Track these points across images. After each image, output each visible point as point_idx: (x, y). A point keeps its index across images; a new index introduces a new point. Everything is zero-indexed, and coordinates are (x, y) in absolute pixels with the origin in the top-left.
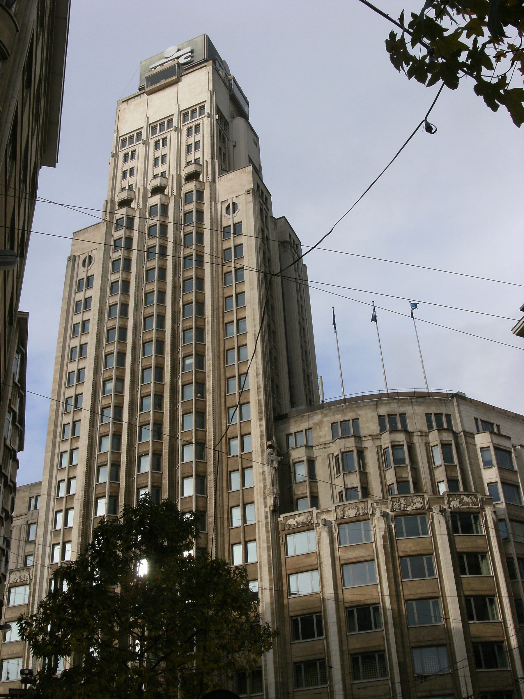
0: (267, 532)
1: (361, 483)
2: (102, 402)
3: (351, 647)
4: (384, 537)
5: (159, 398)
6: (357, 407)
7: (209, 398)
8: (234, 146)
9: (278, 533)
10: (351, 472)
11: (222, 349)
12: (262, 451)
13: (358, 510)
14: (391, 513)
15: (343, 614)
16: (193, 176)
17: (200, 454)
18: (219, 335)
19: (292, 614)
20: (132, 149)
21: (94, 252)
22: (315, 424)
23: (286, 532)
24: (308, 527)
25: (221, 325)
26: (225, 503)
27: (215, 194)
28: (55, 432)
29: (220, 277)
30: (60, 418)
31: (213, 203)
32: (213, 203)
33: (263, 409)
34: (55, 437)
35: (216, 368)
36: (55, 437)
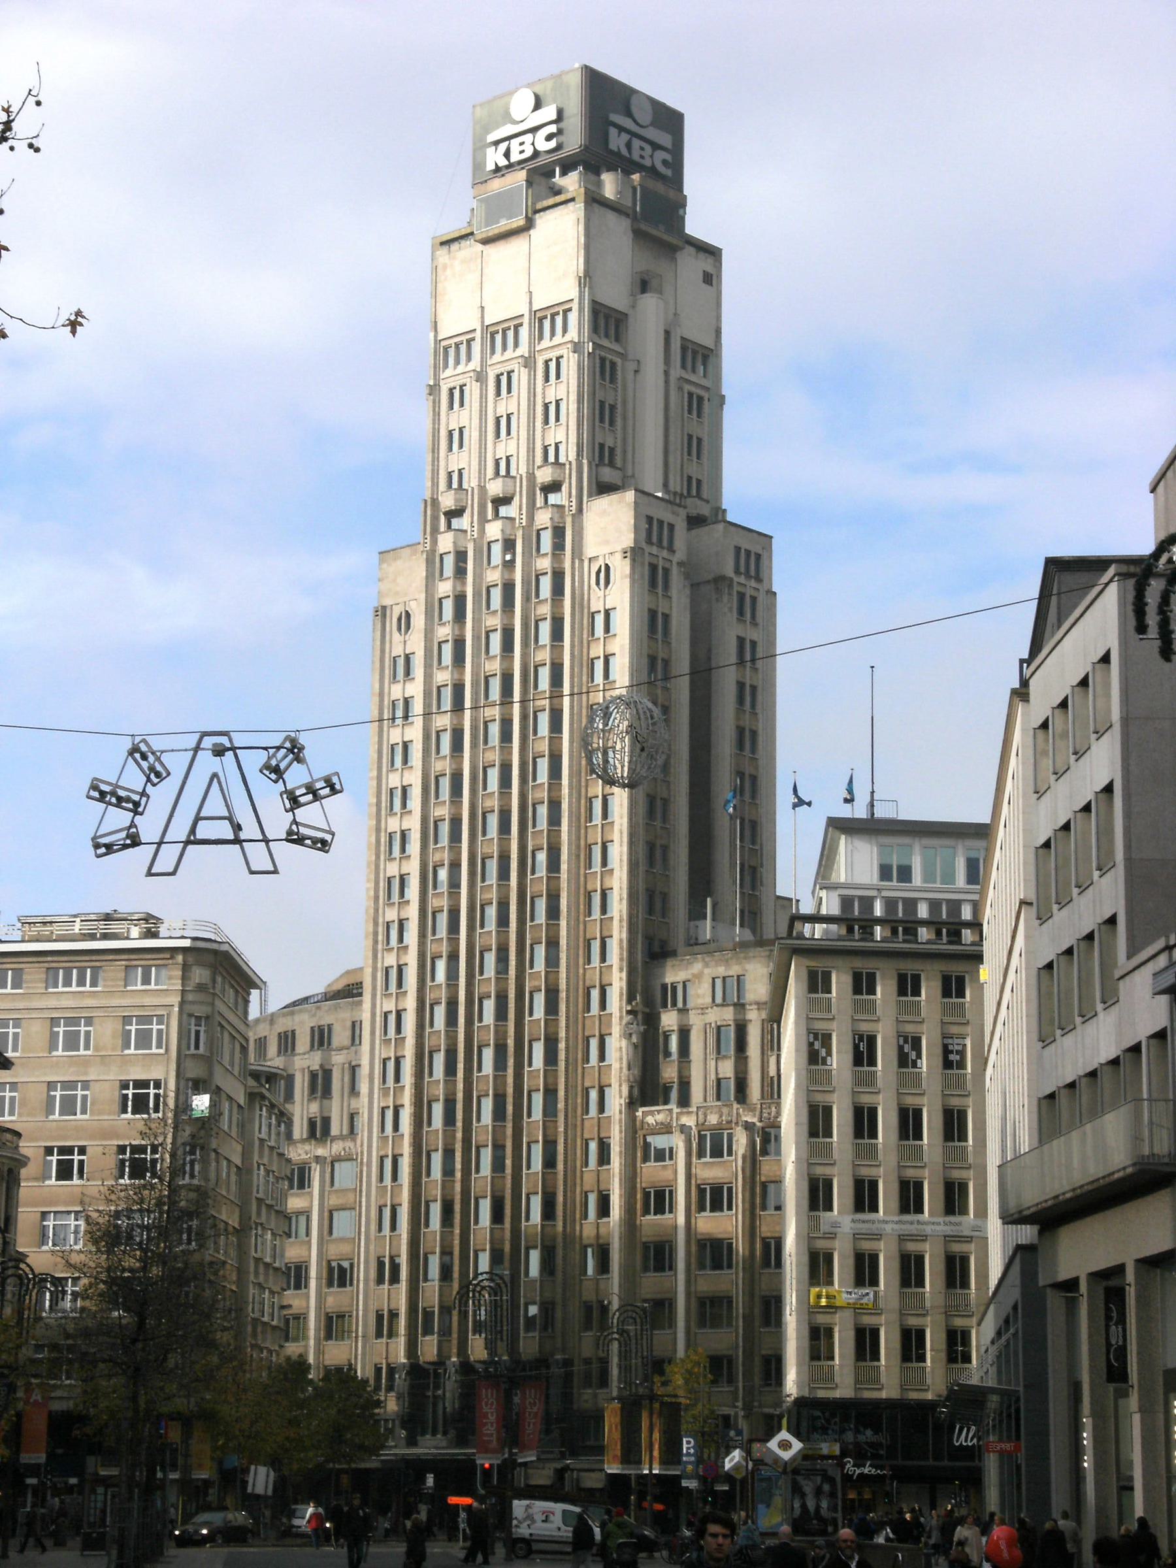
0: (621, 1132)
1: (737, 1072)
2: (433, 903)
3: (700, 1288)
4: (744, 1157)
5: (503, 906)
6: (745, 958)
7: (563, 923)
8: (636, 372)
9: (635, 1132)
10: (725, 1057)
11: (582, 843)
12: (621, 1018)
13: (721, 1116)
14: (758, 1124)
15: (694, 1249)
17: (552, 1007)
18: (579, 819)
19: (644, 1239)
20: (461, 382)
22: (694, 976)
23: (644, 1132)
24: (666, 1129)
25: (583, 801)
26: (579, 1082)
27: (582, 538)
28: (376, 934)
30: (381, 911)
31: (577, 561)
32: (577, 561)
34: (376, 942)
35: (575, 876)
36: (376, 942)
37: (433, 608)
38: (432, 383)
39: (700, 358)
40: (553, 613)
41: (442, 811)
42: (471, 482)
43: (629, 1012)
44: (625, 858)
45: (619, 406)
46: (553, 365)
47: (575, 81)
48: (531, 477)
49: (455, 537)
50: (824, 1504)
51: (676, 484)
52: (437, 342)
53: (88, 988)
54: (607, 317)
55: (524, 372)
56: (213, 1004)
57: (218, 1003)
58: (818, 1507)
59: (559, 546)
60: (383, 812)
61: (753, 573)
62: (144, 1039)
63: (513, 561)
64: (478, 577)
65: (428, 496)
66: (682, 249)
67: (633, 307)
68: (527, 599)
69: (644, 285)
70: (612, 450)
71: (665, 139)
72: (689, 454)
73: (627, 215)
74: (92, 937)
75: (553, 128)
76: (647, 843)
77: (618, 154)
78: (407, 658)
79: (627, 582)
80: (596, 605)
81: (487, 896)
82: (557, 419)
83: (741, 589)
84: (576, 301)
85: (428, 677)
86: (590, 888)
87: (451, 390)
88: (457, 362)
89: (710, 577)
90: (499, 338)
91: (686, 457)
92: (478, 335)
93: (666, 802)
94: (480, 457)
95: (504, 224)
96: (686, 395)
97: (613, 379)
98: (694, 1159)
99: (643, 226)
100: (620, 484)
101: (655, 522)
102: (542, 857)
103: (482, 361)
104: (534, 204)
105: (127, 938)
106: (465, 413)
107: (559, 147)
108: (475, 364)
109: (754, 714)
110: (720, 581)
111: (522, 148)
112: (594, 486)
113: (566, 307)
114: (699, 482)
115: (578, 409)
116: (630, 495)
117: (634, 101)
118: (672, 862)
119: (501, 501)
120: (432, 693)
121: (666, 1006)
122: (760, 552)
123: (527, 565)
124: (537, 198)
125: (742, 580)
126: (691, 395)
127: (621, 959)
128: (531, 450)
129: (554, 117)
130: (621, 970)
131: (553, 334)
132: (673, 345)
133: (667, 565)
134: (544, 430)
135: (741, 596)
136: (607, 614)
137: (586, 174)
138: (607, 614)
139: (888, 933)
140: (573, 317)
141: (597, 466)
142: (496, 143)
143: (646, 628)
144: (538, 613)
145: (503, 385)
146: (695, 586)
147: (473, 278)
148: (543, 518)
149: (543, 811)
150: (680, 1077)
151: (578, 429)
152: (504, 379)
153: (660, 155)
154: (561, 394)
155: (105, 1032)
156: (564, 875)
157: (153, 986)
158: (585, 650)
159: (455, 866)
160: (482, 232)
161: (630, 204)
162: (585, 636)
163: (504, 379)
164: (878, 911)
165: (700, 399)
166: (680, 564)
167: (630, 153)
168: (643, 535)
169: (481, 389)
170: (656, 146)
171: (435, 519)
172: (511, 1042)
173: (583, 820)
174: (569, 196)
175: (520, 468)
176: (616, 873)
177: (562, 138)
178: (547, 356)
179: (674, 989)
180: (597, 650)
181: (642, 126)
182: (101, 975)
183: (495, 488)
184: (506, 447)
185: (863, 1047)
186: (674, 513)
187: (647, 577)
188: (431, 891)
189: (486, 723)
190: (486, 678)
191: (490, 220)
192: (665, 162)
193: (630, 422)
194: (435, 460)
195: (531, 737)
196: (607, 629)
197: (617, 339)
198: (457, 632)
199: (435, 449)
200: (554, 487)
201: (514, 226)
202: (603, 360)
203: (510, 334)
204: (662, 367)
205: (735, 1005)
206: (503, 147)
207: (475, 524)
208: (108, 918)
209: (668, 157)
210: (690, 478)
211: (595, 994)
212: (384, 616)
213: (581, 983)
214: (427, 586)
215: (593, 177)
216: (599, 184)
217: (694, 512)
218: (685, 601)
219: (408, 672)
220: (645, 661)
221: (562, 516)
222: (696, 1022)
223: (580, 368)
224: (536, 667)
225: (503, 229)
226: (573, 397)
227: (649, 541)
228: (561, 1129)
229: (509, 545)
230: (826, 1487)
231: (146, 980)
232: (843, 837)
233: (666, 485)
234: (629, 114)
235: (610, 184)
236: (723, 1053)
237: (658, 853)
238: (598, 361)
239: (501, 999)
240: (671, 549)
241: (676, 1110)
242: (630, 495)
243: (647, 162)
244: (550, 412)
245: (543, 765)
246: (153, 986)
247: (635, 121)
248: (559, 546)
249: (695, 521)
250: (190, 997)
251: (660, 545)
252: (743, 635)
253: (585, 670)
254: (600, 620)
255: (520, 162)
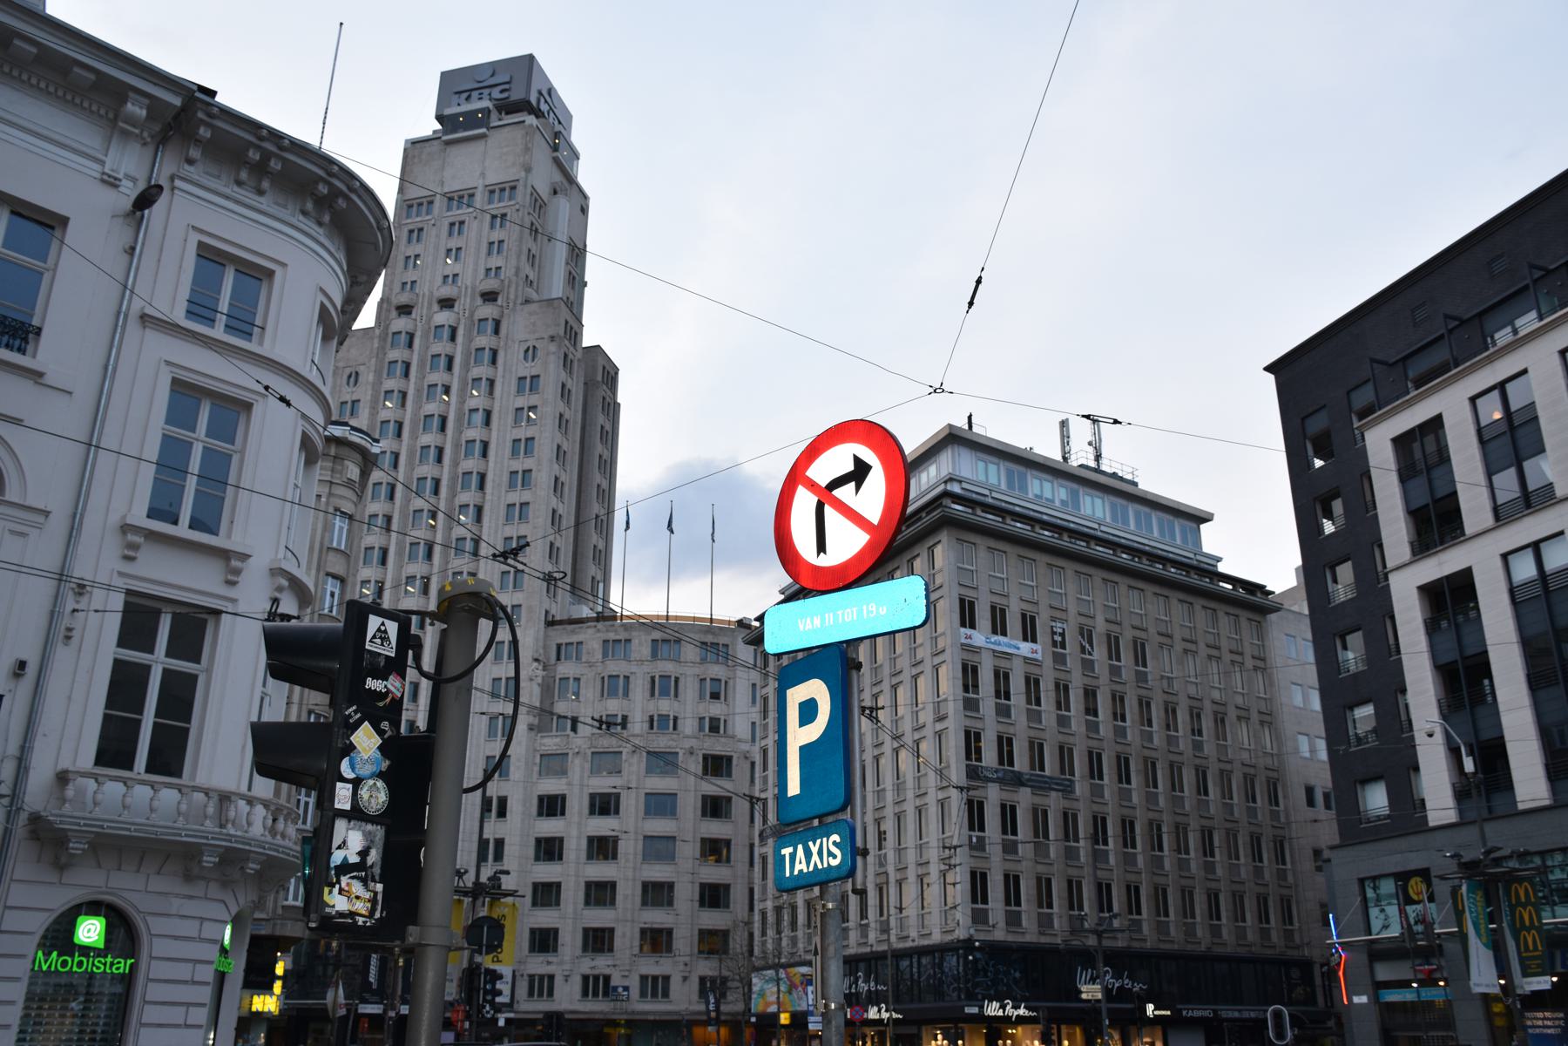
16: (489, 297)
21: (362, 368)
45: (538, 257)
69: (555, 192)
75: (507, 86)
165: (574, 278)
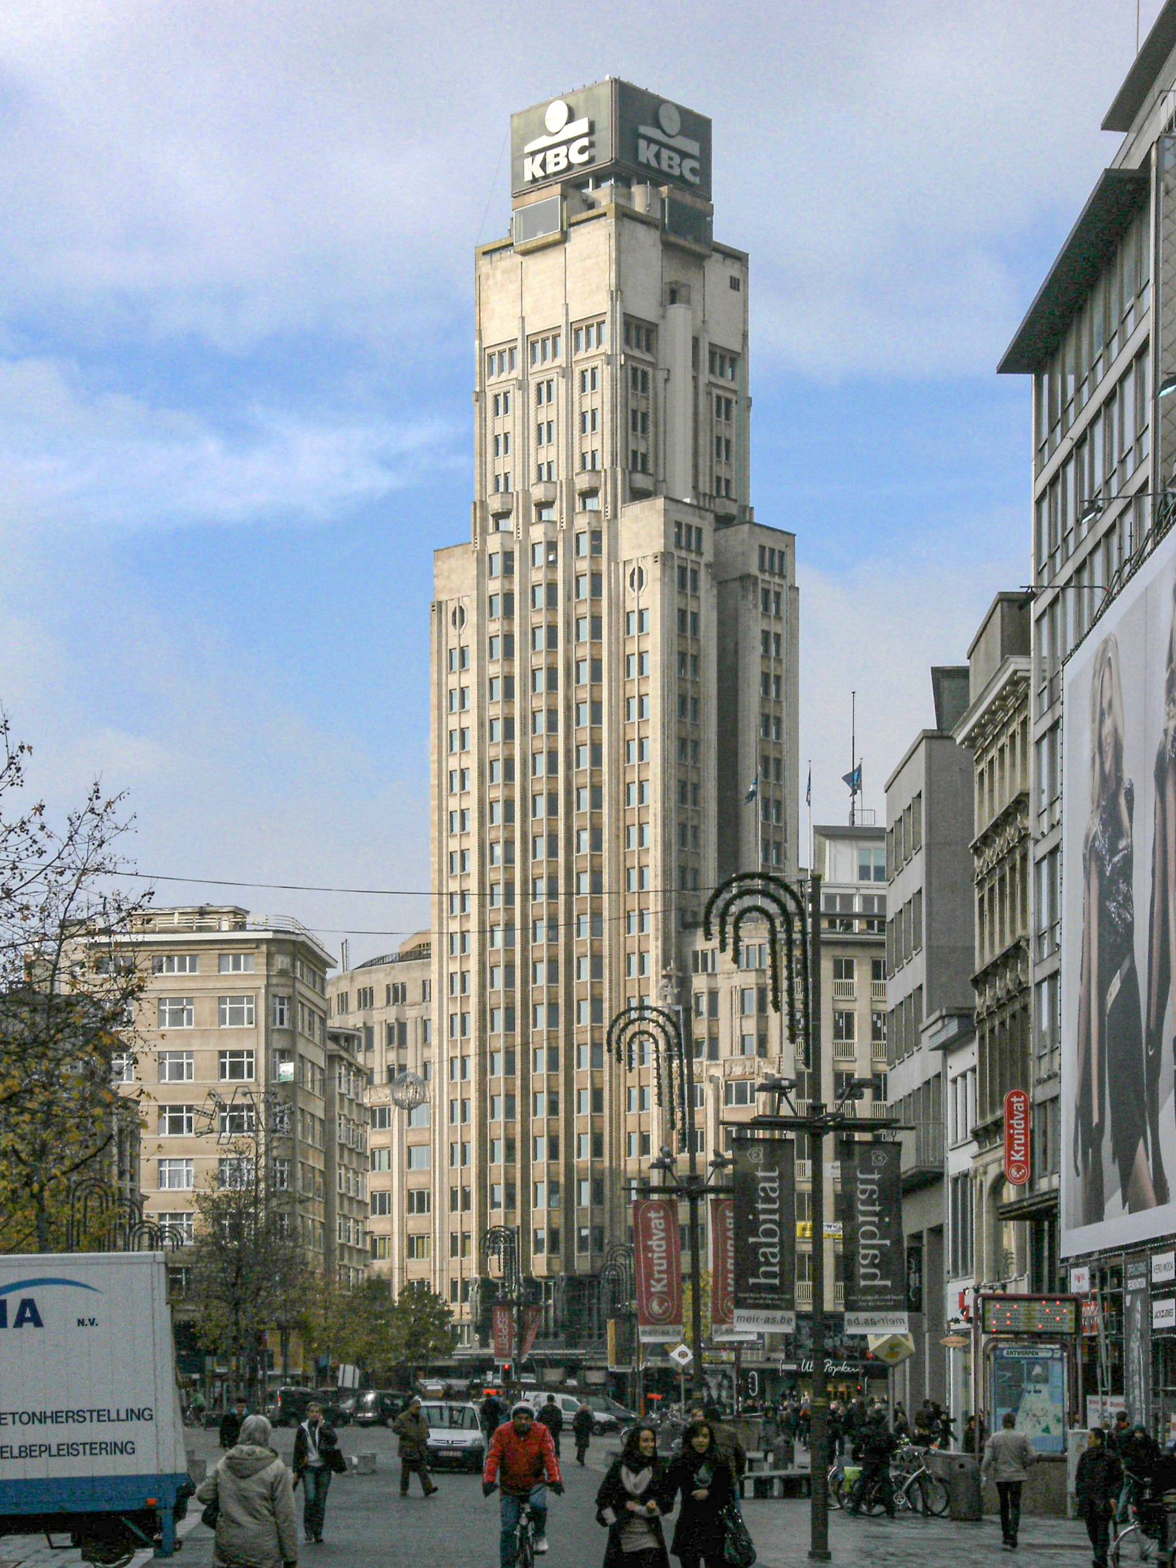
1: (758, 1030)
2: (491, 876)
8: (667, 380)
12: (657, 981)
17: (597, 971)
20: (505, 390)
25: (621, 787)
27: (617, 543)
29: (621, 704)
33: (660, 926)
34: (441, 910)
35: (615, 854)
37: (485, 604)
38: (478, 389)
39: (727, 362)
40: (592, 613)
41: (497, 793)
42: (516, 486)
43: (664, 977)
44: (659, 838)
46: (588, 375)
47: (605, 95)
48: (570, 482)
49: (502, 538)
50: (724, 1394)
51: (705, 486)
52: (482, 350)
53: (187, 973)
54: (638, 328)
55: (562, 381)
56: (294, 986)
57: (298, 986)
58: (719, 1397)
59: (596, 549)
60: (444, 793)
61: (777, 570)
62: (237, 1016)
63: (555, 562)
64: (524, 576)
65: (477, 498)
66: (710, 256)
67: (664, 317)
68: (568, 598)
69: (673, 295)
70: (644, 456)
71: (693, 147)
72: (718, 455)
73: (656, 227)
74: (190, 930)
76: (679, 824)
77: (647, 166)
78: (462, 652)
79: (658, 584)
80: (631, 605)
81: (538, 871)
82: (594, 428)
83: (766, 586)
84: (609, 314)
85: (481, 669)
86: (628, 865)
87: (496, 397)
88: (501, 370)
89: (738, 574)
90: (539, 346)
91: (715, 459)
92: (519, 344)
93: (696, 787)
94: (523, 463)
95: (541, 237)
96: (715, 399)
97: (645, 389)
98: (722, 1106)
99: (672, 238)
100: (651, 488)
101: (684, 528)
102: (586, 837)
103: (523, 371)
104: (568, 217)
105: (219, 931)
106: (509, 419)
107: (591, 160)
108: (517, 373)
109: (778, 702)
110: (745, 578)
111: (557, 160)
112: (628, 492)
113: (600, 319)
114: (728, 482)
115: (612, 419)
116: (660, 502)
117: (663, 112)
118: (702, 842)
119: (542, 505)
120: (486, 685)
121: (697, 971)
122: (783, 549)
123: (567, 567)
124: (572, 211)
125: (767, 577)
126: (719, 398)
127: (657, 930)
128: (570, 457)
129: (586, 130)
130: (657, 939)
131: (588, 345)
132: (701, 352)
133: (696, 567)
134: (581, 438)
135: (766, 592)
136: (641, 613)
137: (617, 187)
138: (641, 613)
139: (865, 926)
140: (606, 330)
141: (630, 472)
142: (533, 154)
143: (676, 628)
144: (579, 612)
145: (544, 392)
146: (721, 585)
147: (514, 287)
148: (582, 523)
149: (586, 795)
150: (710, 1033)
151: (612, 439)
152: (544, 388)
153: (689, 164)
154: (597, 404)
155: (203, 1010)
156: (605, 853)
157: (242, 972)
158: (621, 648)
159: (509, 844)
160: (522, 244)
161: (659, 217)
162: (621, 634)
163: (544, 388)
164: (857, 907)
166: (708, 566)
167: (659, 163)
168: (673, 539)
169: (523, 397)
170: (684, 155)
171: (484, 519)
172: (561, 1001)
173: (621, 803)
174: (601, 211)
175: (560, 474)
176: (652, 851)
177: (593, 151)
178: (583, 367)
179: (705, 956)
180: (632, 648)
181: (669, 136)
182: (198, 962)
183: (538, 493)
184: (547, 454)
185: (842, 1023)
186: (701, 517)
187: (676, 579)
188: (488, 866)
189: (534, 713)
190: (533, 671)
191: (529, 233)
192: (693, 170)
193: (661, 429)
194: (483, 463)
195: (574, 727)
196: (641, 628)
197: (649, 349)
198: (506, 628)
199: (482, 454)
200: (591, 493)
201: (551, 239)
202: (635, 370)
203: (549, 343)
204: (690, 373)
205: (757, 970)
206: (539, 157)
207: (521, 526)
208: (202, 912)
209: (696, 165)
210: (719, 479)
211: (635, 960)
212: (440, 611)
213: (622, 950)
214: (478, 583)
215: (624, 190)
216: (630, 197)
217: (722, 512)
218: (713, 601)
219: (463, 664)
220: (676, 657)
221: (599, 521)
222: (723, 985)
223: (613, 380)
224: (577, 663)
225: (540, 243)
226: (607, 407)
227: (678, 545)
228: (607, 1078)
229: (551, 546)
230: (725, 1382)
231: (236, 966)
232: (828, 842)
233: (695, 487)
234: (658, 125)
235: (640, 198)
236: (747, 1012)
237: (689, 833)
238: (630, 372)
239: (553, 962)
240: (699, 553)
241: (705, 1063)
242: (660, 502)
243: (676, 172)
244: (587, 421)
245: (586, 752)
246: (242, 972)
247: (664, 132)
248: (596, 549)
249: (724, 521)
250: (274, 981)
251: (689, 549)
252: (767, 629)
253: (621, 665)
254: (634, 619)
255: (555, 174)
